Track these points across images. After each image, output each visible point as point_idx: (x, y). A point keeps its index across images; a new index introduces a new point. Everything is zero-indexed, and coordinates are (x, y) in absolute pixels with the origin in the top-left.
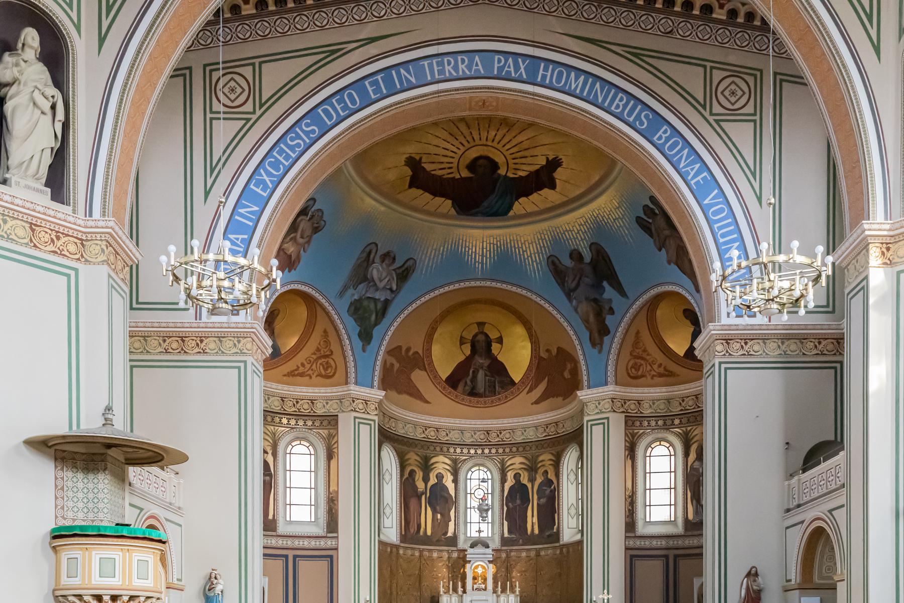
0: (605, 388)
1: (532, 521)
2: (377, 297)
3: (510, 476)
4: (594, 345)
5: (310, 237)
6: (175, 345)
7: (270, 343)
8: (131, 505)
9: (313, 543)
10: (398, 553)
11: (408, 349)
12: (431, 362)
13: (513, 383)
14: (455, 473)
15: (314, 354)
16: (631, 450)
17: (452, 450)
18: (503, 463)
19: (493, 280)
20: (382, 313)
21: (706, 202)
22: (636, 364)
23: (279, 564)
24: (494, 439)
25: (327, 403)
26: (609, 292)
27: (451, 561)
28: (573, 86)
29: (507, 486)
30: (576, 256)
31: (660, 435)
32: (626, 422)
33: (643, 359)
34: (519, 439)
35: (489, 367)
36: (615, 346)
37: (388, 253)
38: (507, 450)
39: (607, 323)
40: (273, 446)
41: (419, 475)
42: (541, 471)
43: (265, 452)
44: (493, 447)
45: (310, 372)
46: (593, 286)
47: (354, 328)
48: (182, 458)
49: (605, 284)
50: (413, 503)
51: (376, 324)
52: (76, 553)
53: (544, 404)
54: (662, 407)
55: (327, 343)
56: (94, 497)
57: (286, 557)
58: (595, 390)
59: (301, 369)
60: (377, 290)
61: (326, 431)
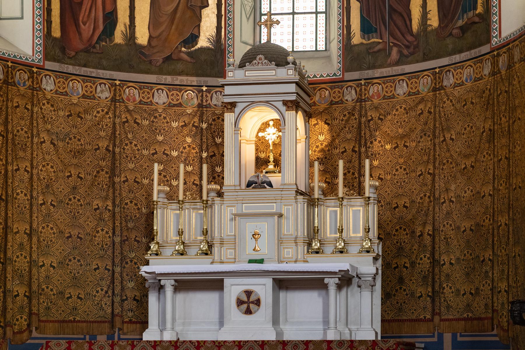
10: (36, 88)
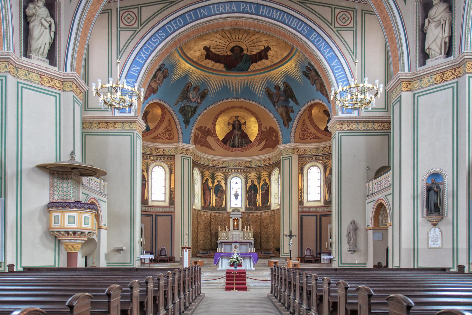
0: (290, 144)
3: (249, 181)
4: (285, 126)
5: (163, 80)
6: (104, 126)
7: (145, 125)
8: (83, 193)
9: (164, 210)
11: (205, 128)
12: (215, 133)
13: (251, 142)
14: (226, 180)
16: (301, 170)
17: (224, 170)
19: (241, 98)
21: (332, 65)
23: (149, 218)
24: (243, 166)
26: (292, 103)
28: (275, 16)
30: (277, 88)
33: (306, 131)
34: (253, 165)
38: (248, 170)
40: (146, 169)
42: (262, 179)
43: (143, 171)
44: (242, 169)
45: (163, 137)
46: (285, 100)
47: (182, 119)
48: (104, 174)
49: (290, 99)
51: (191, 117)
52: (58, 214)
55: (170, 125)
56: (67, 191)
57: (152, 215)
58: (285, 145)
59: (159, 136)
61: (170, 162)
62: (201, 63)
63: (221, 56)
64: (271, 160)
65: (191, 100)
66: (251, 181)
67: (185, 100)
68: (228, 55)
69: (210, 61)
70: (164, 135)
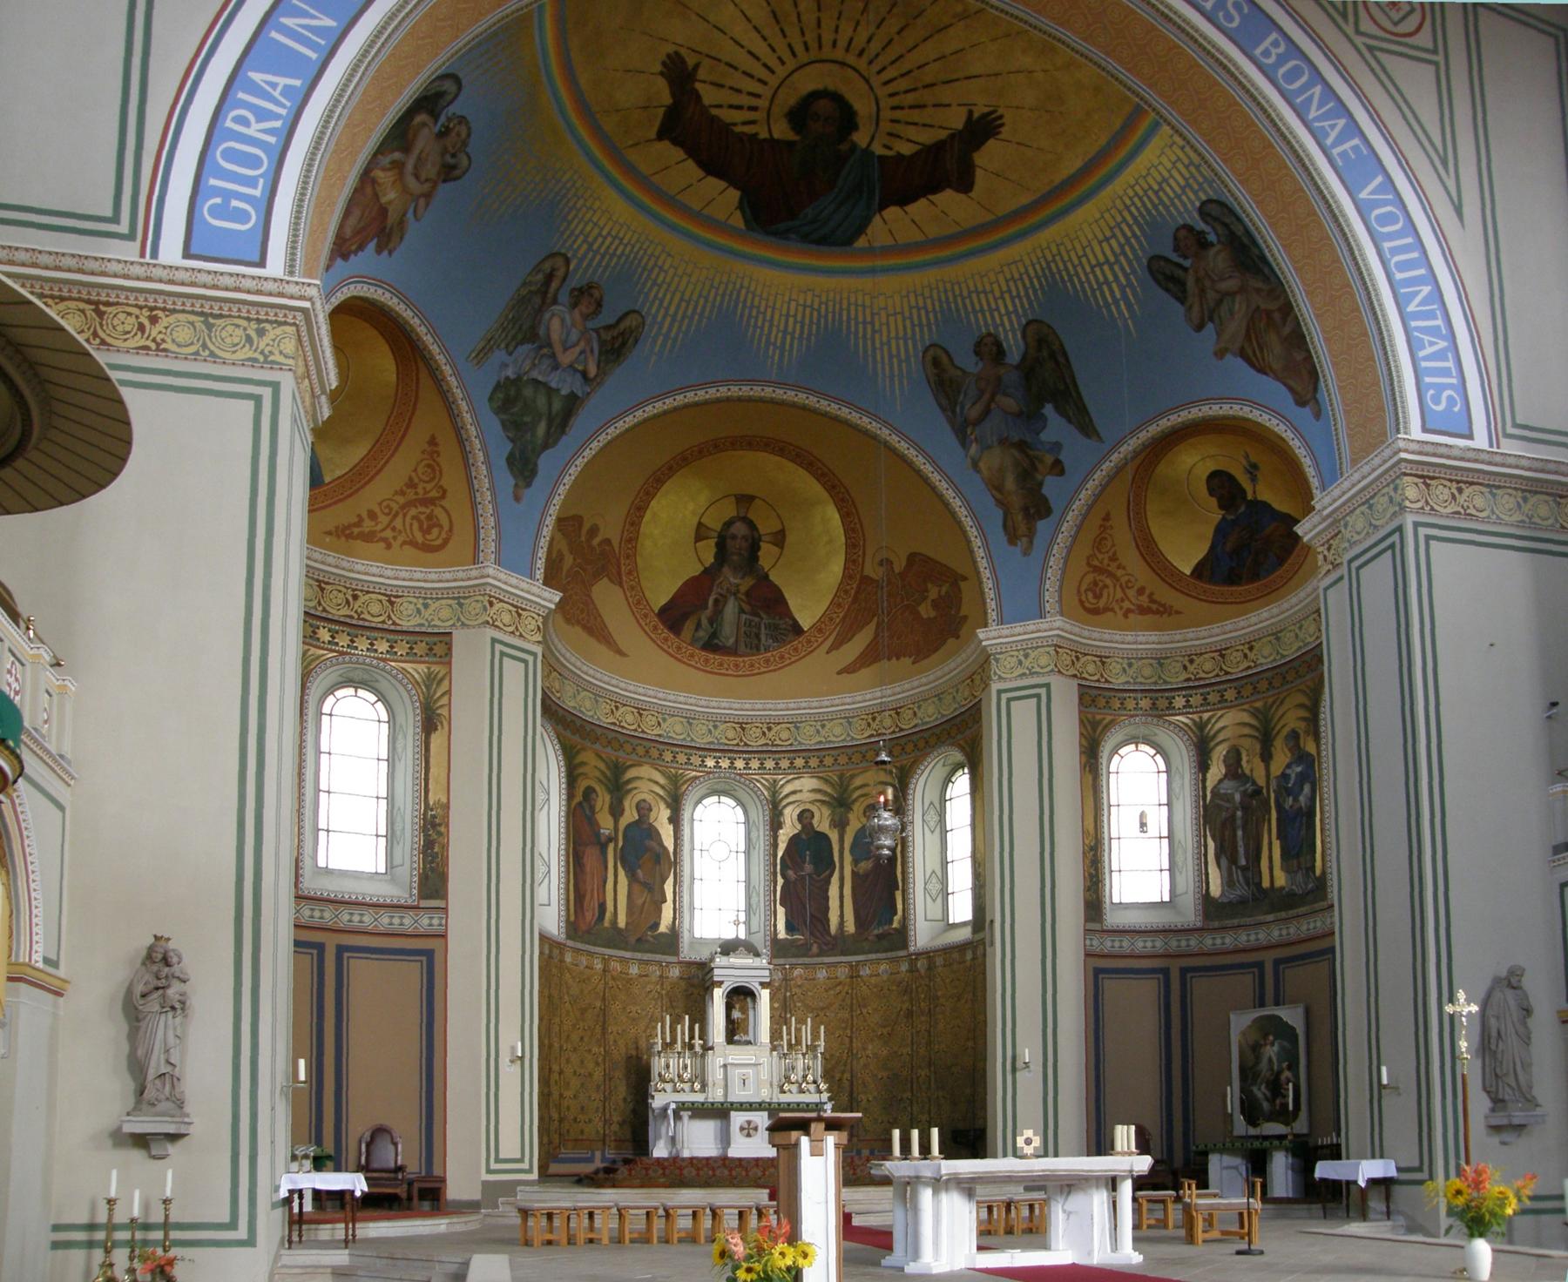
0: (1043, 624)
1: (840, 909)
2: (553, 385)
3: (790, 815)
4: (1012, 538)
5: (435, 184)
13: (797, 630)
15: (402, 493)
18: (774, 789)
20: (561, 421)
22: (1095, 583)
25: (426, 606)
26: (1056, 428)
27: (667, 986)
29: (785, 835)
31: (1143, 730)
32: (1081, 699)
33: (1111, 575)
35: (747, 594)
36: (1063, 539)
37: (590, 286)
38: (785, 764)
39: (1045, 491)
41: (603, 800)
42: (858, 808)
44: (742, 761)
45: (388, 534)
46: (1020, 415)
47: (502, 447)
49: (1048, 410)
50: (591, 857)
53: (865, 673)
54: (1147, 672)
55: (434, 470)
58: (1018, 628)
59: (368, 525)
60: (556, 367)
61: (422, 668)
62: (633, 156)
63: (741, 137)
64: (907, 714)
65: (553, 356)
66: (800, 817)
67: (526, 347)
68: (772, 142)
69: (677, 153)
70: (398, 523)
